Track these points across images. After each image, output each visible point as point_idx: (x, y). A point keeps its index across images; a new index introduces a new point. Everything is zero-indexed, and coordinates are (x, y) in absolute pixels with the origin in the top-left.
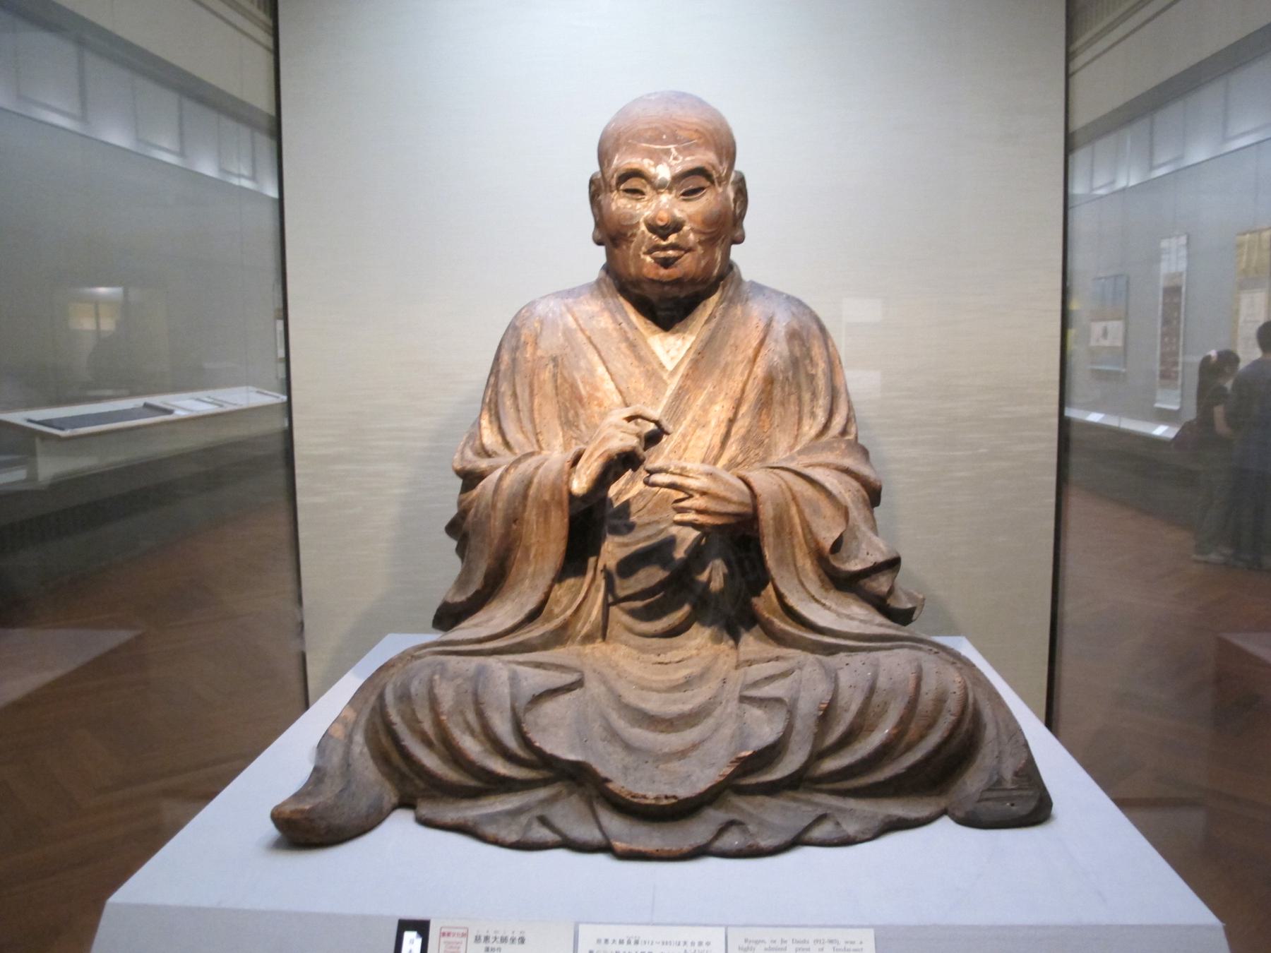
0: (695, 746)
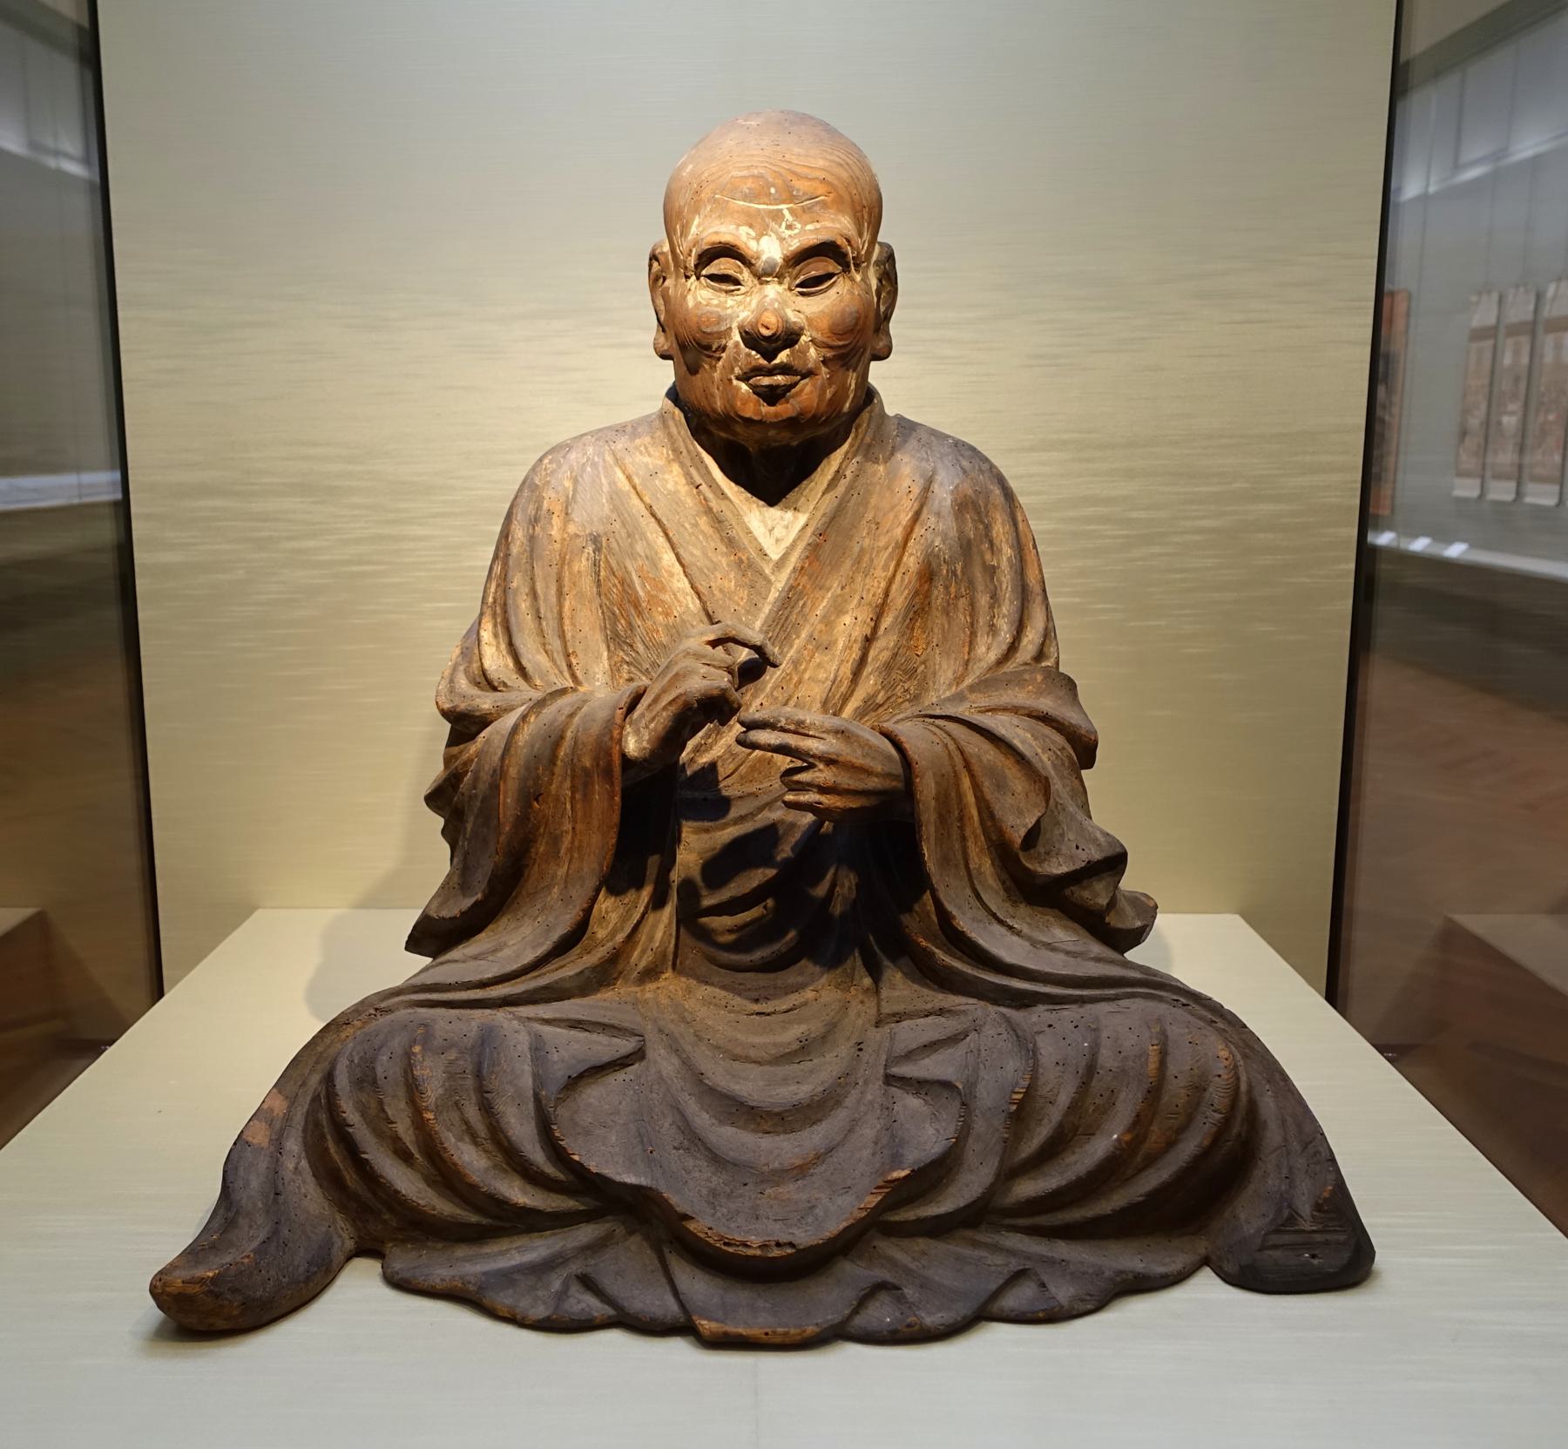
0: (820, 1158)
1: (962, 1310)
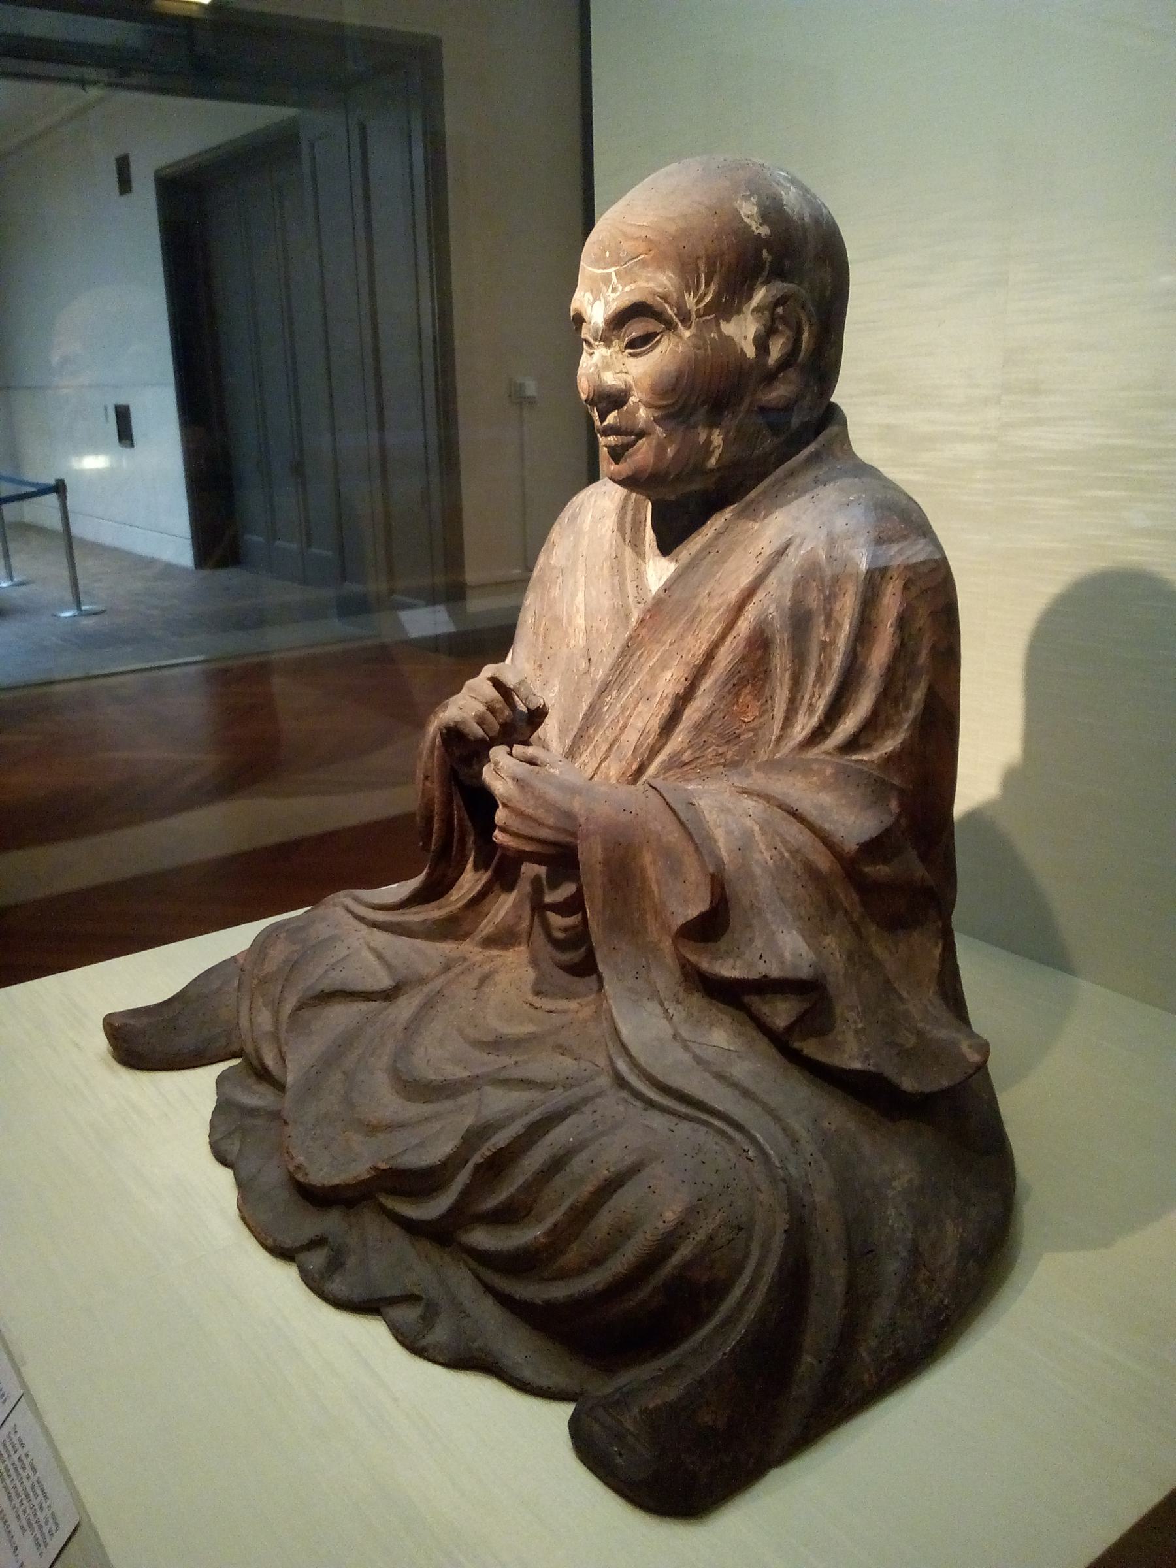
1: (357, 1294)
